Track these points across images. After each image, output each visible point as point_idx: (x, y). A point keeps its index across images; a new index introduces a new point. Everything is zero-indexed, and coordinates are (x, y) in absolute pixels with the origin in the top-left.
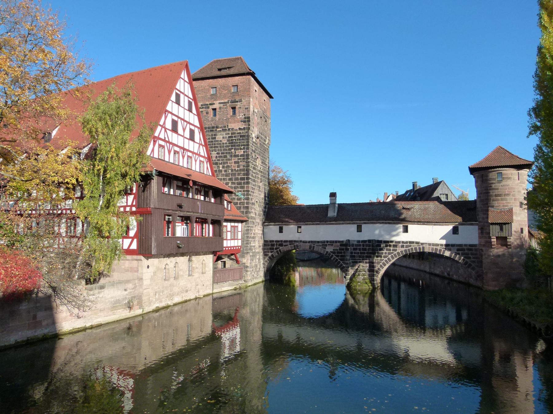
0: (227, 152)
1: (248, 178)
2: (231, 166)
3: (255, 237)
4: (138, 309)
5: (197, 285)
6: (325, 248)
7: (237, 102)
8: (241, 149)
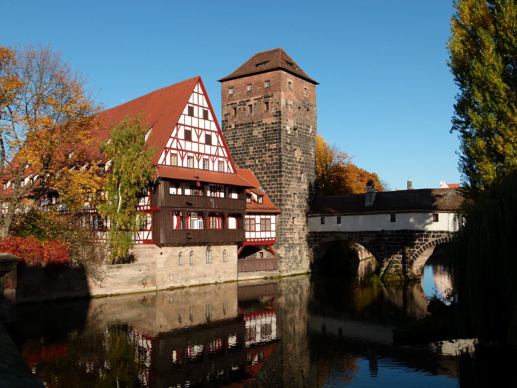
0: (262, 146)
1: (281, 172)
2: (266, 160)
3: (293, 229)
4: (152, 286)
5: (218, 272)
6: (362, 239)
7: (269, 97)
8: (274, 143)
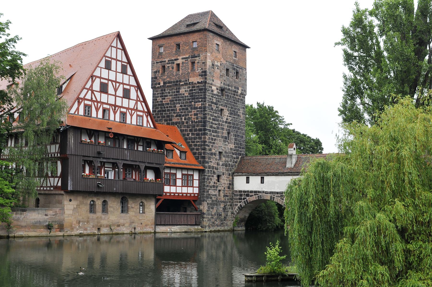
1: (205, 130)
2: (192, 117)
3: (217, 187)
5: (133, 223)
7: (196, 57)
8: (199, 102)
